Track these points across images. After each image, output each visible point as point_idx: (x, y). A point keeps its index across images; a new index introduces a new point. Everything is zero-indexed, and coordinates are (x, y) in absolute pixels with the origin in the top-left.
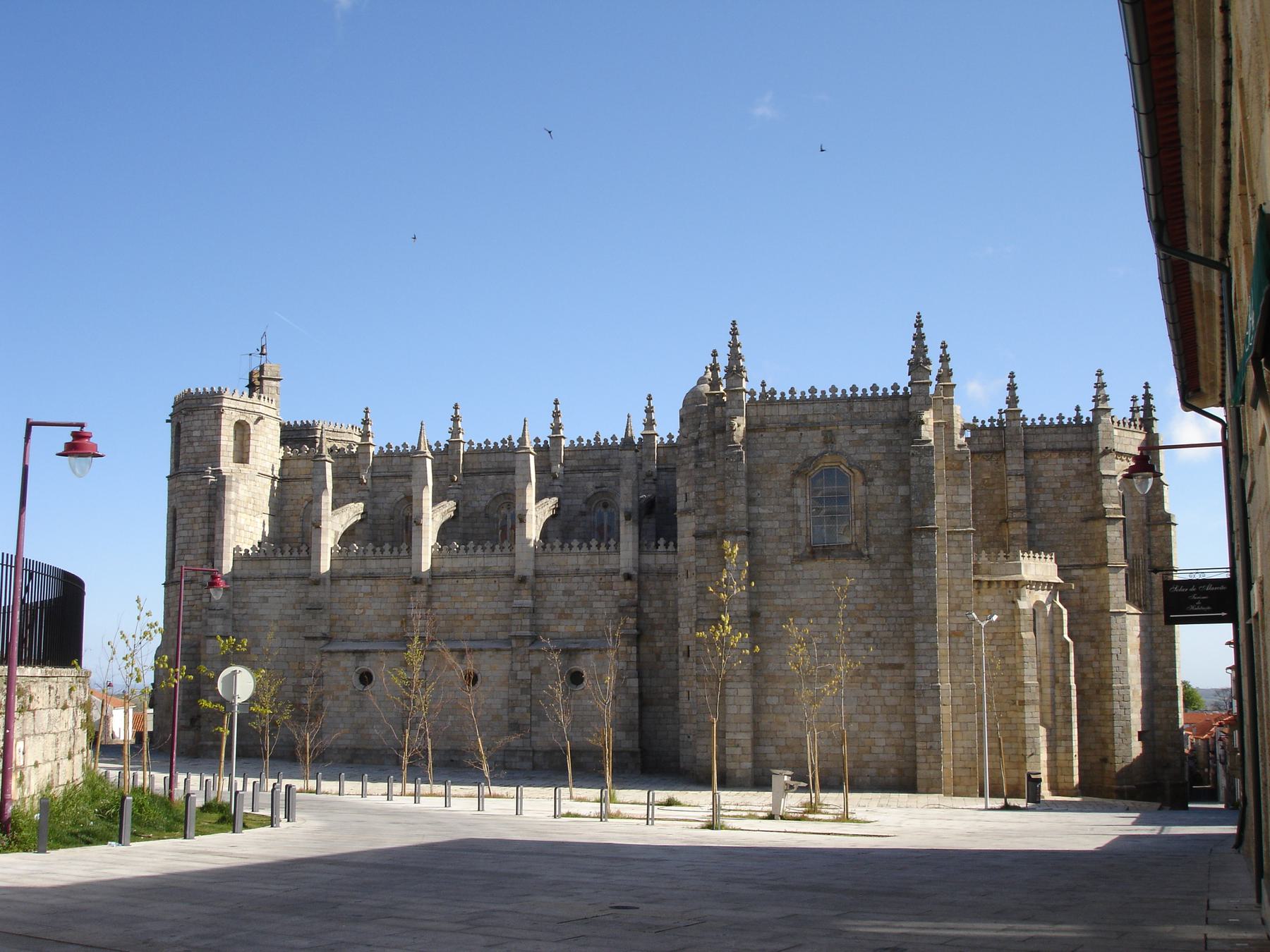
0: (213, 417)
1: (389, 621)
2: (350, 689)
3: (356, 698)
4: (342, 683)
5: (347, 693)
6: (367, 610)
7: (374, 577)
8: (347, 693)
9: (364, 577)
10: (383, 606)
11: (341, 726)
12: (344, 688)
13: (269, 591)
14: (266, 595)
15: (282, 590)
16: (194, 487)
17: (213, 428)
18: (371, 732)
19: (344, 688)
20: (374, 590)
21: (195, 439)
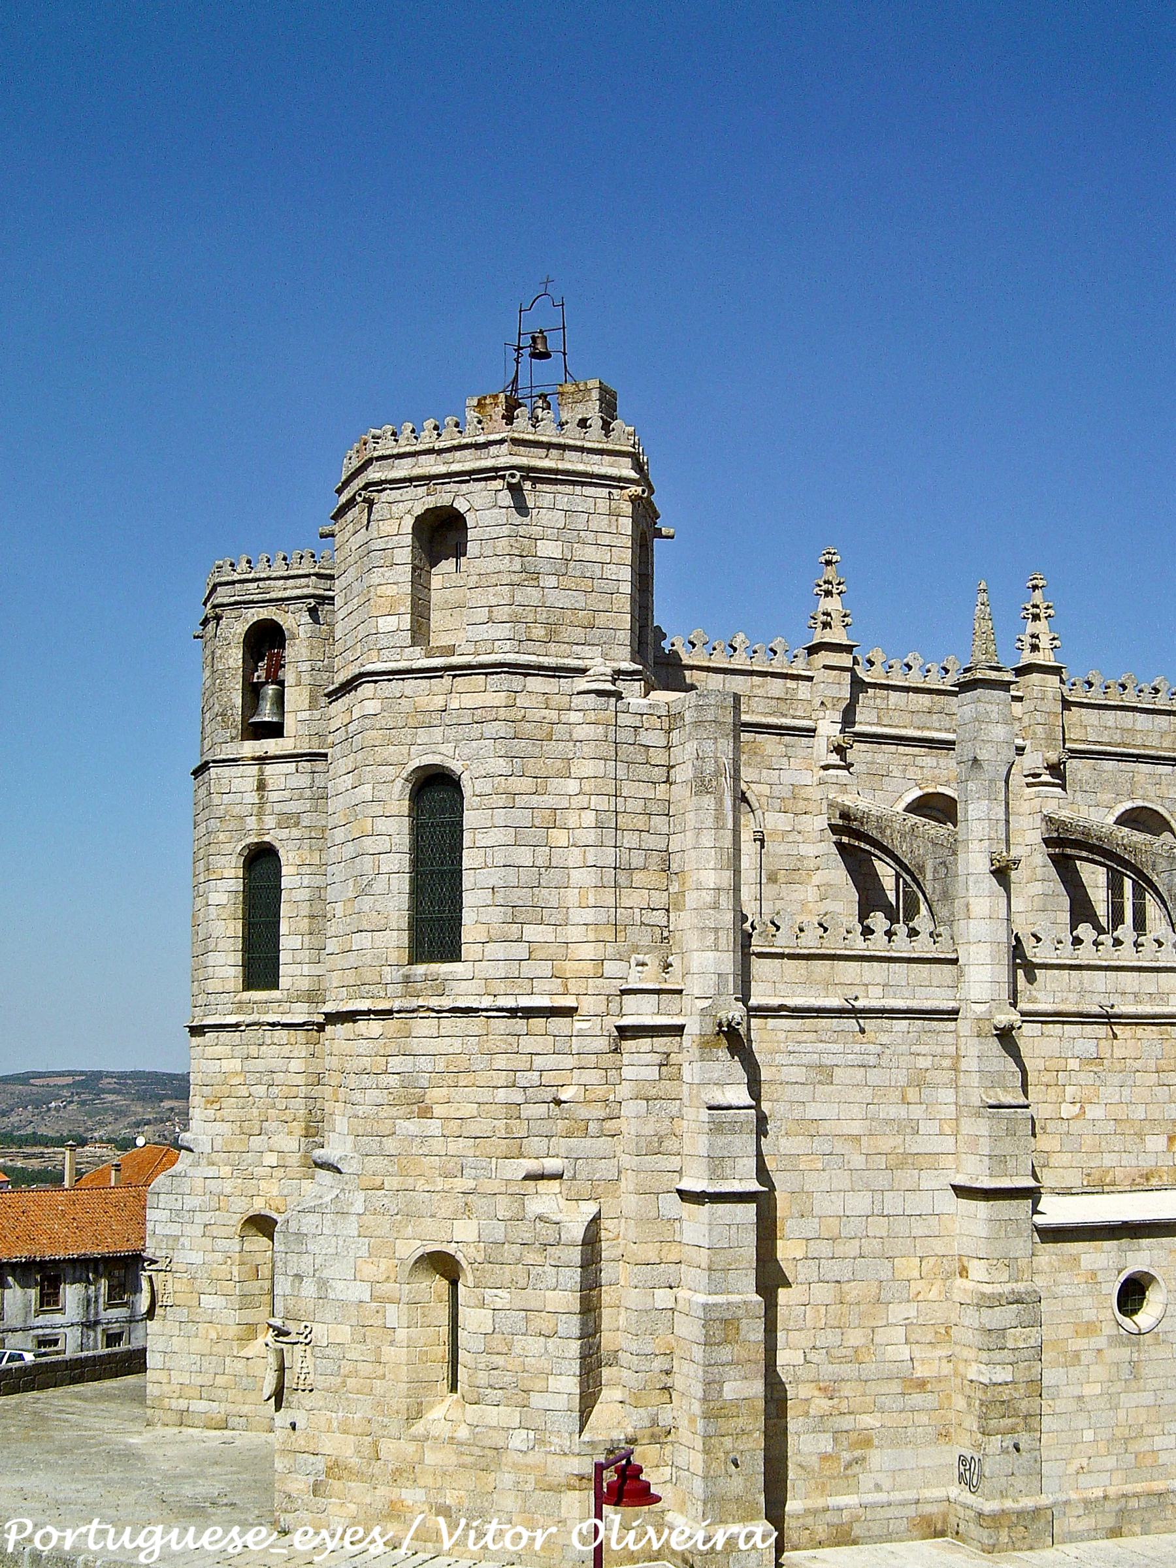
0: (603, 506)
1: (1140, 1135)
2: (1109, 1329)
3: (1124, 1353)
4: (1089, 1315)
5: (1101, 1342)
6: (1088, 1107)
7: (1109, 1019)
8: (1101, 1342)
9: (1083, 1018)
10: (1126, 1091)
11: (1088, 1435)
12: (1090, 1329)
13: (834, 1047)
14: (828, 1060)
15: (872, 1048)
16: (553, 715)
17: (605, 539)
18: (1159, 1442)
19: (1090, 1329)
20: (1105, 1051)
21: (546, 567)
